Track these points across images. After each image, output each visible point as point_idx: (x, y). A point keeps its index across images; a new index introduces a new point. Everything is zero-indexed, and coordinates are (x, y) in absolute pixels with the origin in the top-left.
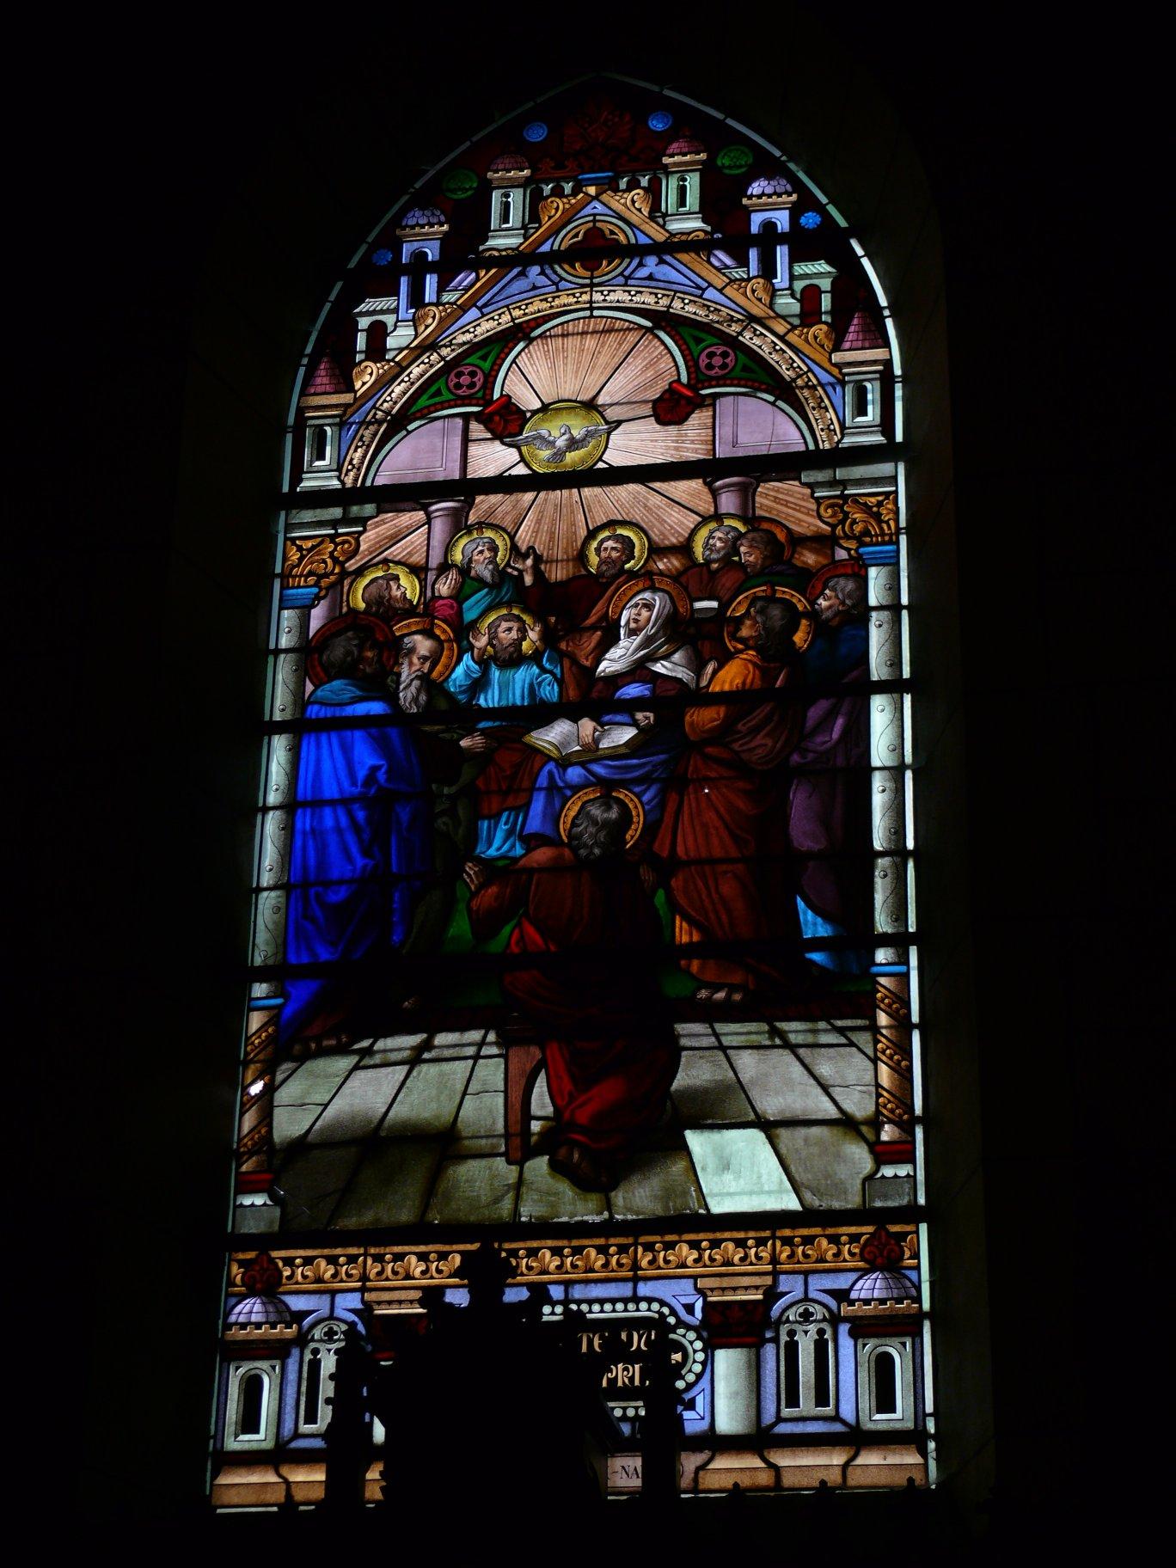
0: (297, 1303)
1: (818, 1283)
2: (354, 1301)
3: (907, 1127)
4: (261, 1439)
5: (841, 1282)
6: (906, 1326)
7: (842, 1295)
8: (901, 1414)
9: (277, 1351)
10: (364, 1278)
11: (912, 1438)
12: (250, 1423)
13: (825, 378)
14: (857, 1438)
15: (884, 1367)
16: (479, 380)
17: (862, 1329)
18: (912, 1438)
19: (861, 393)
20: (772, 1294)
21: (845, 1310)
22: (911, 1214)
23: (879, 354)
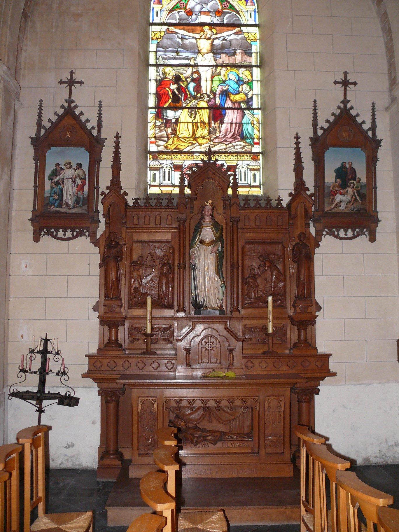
0: (161, 162)
1: (245, 162)
2: (170, 162)
3: (259, 139)
4: (157, 183)
5: (248, 162)
6: (258, 170)
7: (248, 165)
8: (257, 184)
9: (158, 169)
10: (172, 158)
11: (259, 186)
12: (155, 180)
13: (244, 10)
14: (250, 186)
15: (255, 175)
16: (185, 5)
17: (251, 170)
18: (259, 186)
19: (251, 14)
20: (237, 164)
21: (249, 167)
22: (259, 153)
23: (254, 7)
